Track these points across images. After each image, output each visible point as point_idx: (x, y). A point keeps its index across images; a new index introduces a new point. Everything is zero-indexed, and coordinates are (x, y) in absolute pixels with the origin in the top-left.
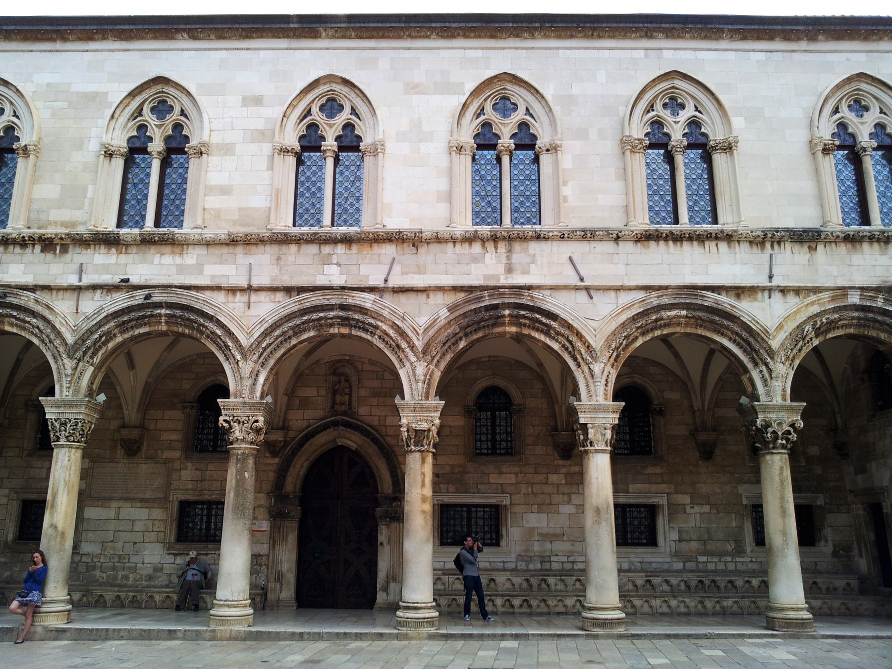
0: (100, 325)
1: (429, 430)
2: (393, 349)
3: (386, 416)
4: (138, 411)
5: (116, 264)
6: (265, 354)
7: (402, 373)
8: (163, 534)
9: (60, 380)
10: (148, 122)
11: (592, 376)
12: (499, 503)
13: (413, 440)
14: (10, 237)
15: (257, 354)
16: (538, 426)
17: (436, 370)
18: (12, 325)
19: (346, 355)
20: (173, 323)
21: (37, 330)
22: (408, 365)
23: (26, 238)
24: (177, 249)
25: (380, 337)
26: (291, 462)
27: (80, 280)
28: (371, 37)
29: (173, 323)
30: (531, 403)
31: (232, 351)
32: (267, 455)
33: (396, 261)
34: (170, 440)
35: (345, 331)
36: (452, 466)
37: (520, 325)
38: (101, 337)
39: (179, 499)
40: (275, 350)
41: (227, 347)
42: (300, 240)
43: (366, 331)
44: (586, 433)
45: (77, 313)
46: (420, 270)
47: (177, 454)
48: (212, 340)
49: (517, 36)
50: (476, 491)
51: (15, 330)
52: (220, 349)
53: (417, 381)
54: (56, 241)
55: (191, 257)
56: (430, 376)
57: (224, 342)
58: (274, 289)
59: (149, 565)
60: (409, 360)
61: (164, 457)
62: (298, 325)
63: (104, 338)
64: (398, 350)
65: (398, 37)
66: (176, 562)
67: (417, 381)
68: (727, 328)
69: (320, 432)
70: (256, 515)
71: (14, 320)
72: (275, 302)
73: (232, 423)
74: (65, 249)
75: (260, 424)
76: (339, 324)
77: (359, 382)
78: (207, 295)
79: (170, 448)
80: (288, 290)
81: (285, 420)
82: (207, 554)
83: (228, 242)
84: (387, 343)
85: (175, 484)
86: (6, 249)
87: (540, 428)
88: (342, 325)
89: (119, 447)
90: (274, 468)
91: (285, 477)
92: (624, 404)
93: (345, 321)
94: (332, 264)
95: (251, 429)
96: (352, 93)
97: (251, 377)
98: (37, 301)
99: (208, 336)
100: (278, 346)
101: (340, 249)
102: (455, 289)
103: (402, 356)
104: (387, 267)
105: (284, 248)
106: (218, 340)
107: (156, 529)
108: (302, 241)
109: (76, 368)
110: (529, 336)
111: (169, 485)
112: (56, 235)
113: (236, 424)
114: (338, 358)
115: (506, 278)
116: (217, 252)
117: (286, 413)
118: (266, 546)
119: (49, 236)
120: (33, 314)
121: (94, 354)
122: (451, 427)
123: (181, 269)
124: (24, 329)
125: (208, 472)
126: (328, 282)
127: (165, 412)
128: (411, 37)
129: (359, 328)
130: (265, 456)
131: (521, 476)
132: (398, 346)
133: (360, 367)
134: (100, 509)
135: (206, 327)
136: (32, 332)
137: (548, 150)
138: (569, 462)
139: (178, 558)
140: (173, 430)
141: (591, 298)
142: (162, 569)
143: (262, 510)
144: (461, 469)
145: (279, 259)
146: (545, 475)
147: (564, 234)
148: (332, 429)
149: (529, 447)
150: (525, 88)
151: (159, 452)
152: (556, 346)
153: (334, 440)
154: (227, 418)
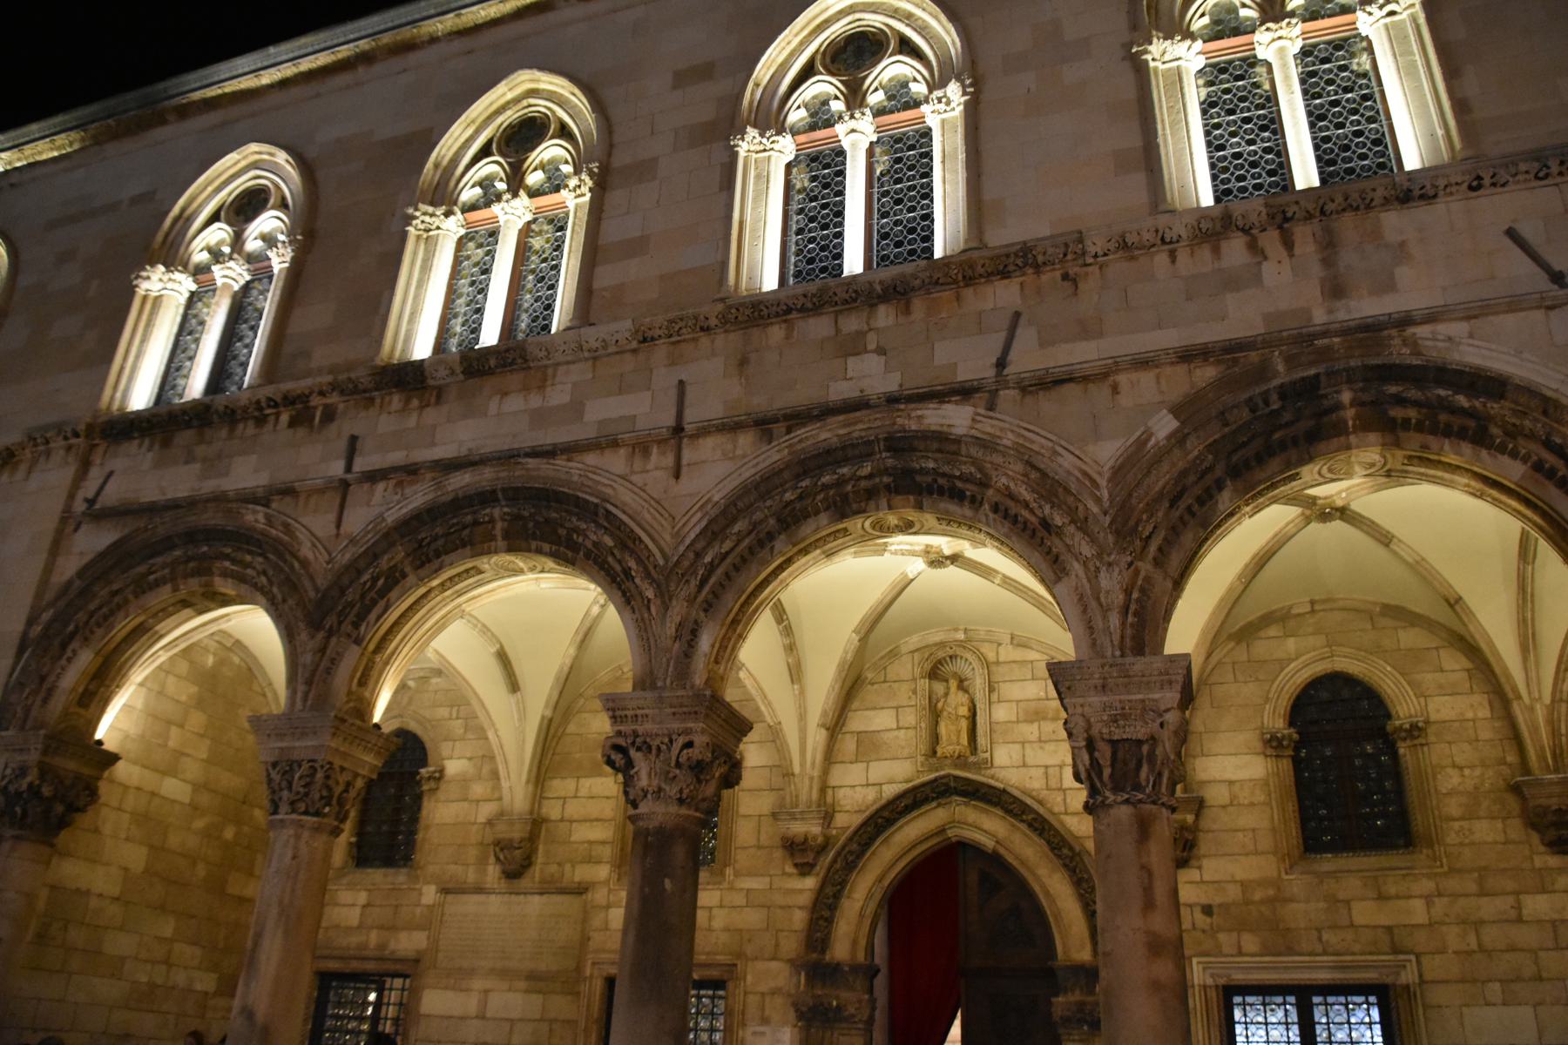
0: (372, 555)
1: (1153, 739)
4: (528, 782)
6: (712, 580)
12: (1389, 980)
13: (1107, 772)
15: (694, 583)
16: (1472, 767)
17: (1158, 576)
19: (956, 630)
21: (263, 579)
23: (264, 404)
25: (995, 508)
26: (843, 884)
30: (1442, 708)
31: (637, 581)
32: (789, 869)
33: (1022, 321)
34: (591, 843)
36: (1244, 885)
38: (375, 580)
39: (605, 974)
40: (737, 568)
41: (627, 572)
42: (789, 311)
46: (1087, 330)
47: (603, 872)
50: (1319, 948)
53: (1105, 611)
56: (1143, 590)
57: (619, 562)
58: (730, 427)
60: (1077, 556)
61: (577, 879)
62: (788, 503)
63: (381, 582)
64: (1046, 534)
67: (1105, 611)
69: (909, 809)
70: (767, 1013)
71: (227, 564)
73: (632, 752)
74: (329, 415)
77: (992, 689)
78: (591, 459)
79: (590, 860)
80: (764, 425)
81: (823, 789)
83: (634, 344)
84: (1015, 520)
86: (232, 430)
87: (1478, 772)
88: (898, 491)
89: (492, 859)
90: (805, 899)
91: (830, 921)
94: (866, 352)
95: (678, 765)
97: (677, 637)
100: (744, 560)
101: (885, 316)
102: (1188, 356)
103: (1057, 545)
104: (1003, 335)
106: (610, 559)
108: (794, 315)
109: (323, 650)
113: (639, 755)
114: (938, 638)
115: (1330, 312)
117: (826, 772)
122: (1231, 783)
123: (539, 418)
126: (857, 394)
127: (582, 781)
129: (941, 492)
131: (1440, 904)
132: (1046, 524)
133: (991, 656)
134: (450, 994)
140: (597, 820)
143: (779, 1000)
144: (1271, 892)
145: (743, 362)
146: (1511, 900)
147: (1479, 178)
148: (934, 804)
149: (1456, 825)
153: (941, 831)
154: (621, 741)
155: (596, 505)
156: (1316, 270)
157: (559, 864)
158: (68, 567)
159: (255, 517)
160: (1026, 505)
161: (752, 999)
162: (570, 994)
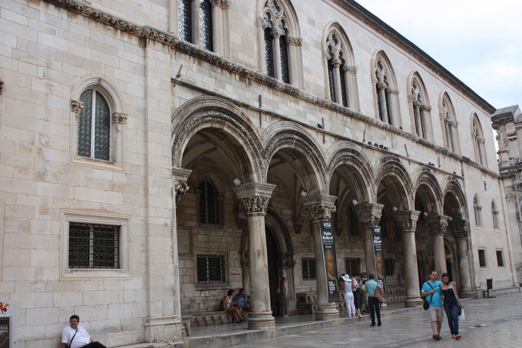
2: (366, 177)
3: (282, 209)
5: (273, 100)
7: (368, 188)
8: (193, 277)
9: (257, 171)
10: (271, 12)
11: (413, 199)
14: (228, 64)
18: (229, 127)
20: (298, 145)
22: (371, 186)
23: (236, 69)
24: (296, 99)
25: (362, 170)
27: (260, 106)
28: (346, 9)
29: (298, 145)
32: (237, 227)
34: (190, 214)
35: (351, 164)
37: (396, 172)
39: (197, 254)
43: (358, 165)
44: (411, 224)
45: (260, 127)
47: (194, 224)
48: (312, 158)
49: (383, 34)
51: (229, 131)
52: (316, 164)
54: (248, 76)
55: (302, 106)
59: (187, 299)
61: (188, 225)
64: (367, 176)
65: (353, 14)
66: (201, 296)
68: (434, 184)
71: (231, 124)
72: (331, 142)
75: (335, 210)
76: (351, 160)
78: (309, 131)
79: (191, 220)
82: (215, 290)
84: (364, 173)
85: (196, 244)
90: (240, 235)
92: (421, 212)
93: (353, 159)
94: (347, 127)
95: (331, 211)
96: (341, 36)
98: (242, 114)
99: (311, 156)
101: (349, 120)
103: (369, 181)
105: (332, 112)
107: (189, 274)
110: (397, 178)
111: (191, 244)
112: (251, 72)
115: (392, 150)
116: (310, 107)
118: (241, 283)
119: (248, 71)
120: (241, 121)
121: (270, 156)
124: (236, 132)
125: (211, 236)
128: (357, 17)
129: (356, 163)
130: (236, 228)
132: (368, 175)
135: (311, 150)
136: (240, 136)
137: (394, 93)
138: (339, 238)
139: (202, 292)
140: (192, 207)
141: (410, 164)
142: (195, 301)
145: (331, 119)
150: (386, 60)
151: (185, 221)
152: (403, 184)
155: (314, 145)
156: (391, 142)
157: (183, 220)
158: (178, 104)
159: (239, 111)
160: (367, 171)
161: (232, 261)
162: (191, 260)
